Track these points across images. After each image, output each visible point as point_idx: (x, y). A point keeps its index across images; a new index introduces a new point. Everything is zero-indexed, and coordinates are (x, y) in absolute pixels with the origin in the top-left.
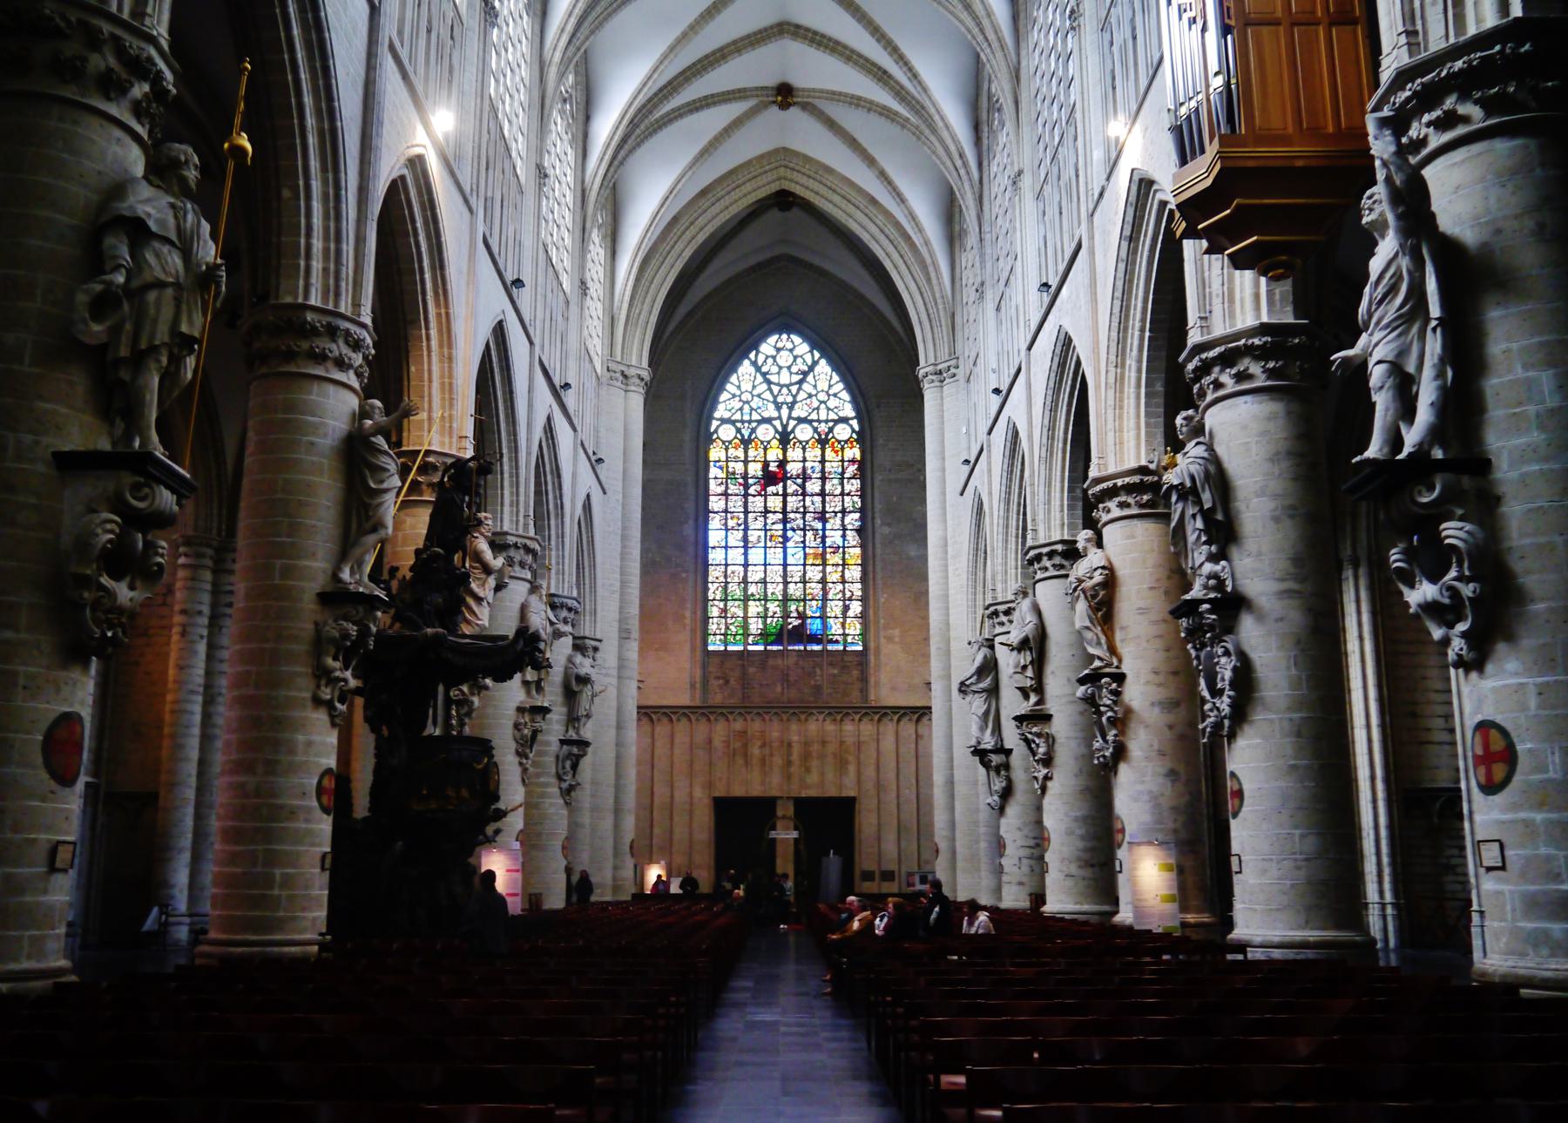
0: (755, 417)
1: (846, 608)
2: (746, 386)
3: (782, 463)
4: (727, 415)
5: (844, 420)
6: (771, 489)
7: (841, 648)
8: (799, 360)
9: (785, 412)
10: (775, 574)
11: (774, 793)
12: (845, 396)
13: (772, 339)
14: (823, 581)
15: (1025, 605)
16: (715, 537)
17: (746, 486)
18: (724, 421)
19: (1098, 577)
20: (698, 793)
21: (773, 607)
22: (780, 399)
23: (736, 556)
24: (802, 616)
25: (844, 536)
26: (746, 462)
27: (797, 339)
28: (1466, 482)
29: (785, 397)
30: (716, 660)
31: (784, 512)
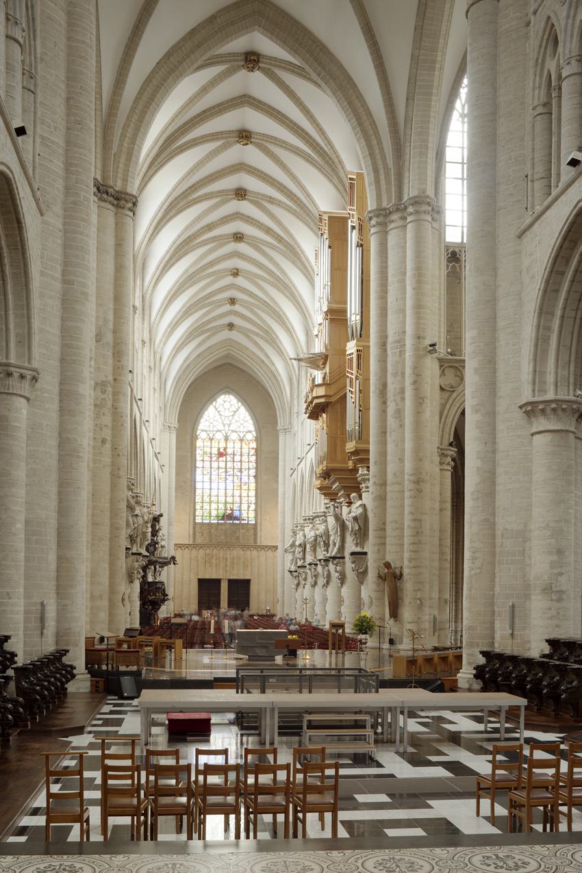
0: (215, 429)
1: (249, 507)
2: (212, 416)
3: (225, 449)
4: (203, 428)
5: (250, 432)
6: (221, 459)
7: (246, 522)
8: (233, 406)
9: (227, 427)
10: (222, 492)
11: (220, 578)
12: (251, 422)
13: (222, 397)
14: (240, 496)
15: (301, 533)
16: (199, 477)
17: (211, 457)
18: (202, 431)
19: (313, 539)
20: (192, 576)
21: (221, 506)
22: (225, 422)
23: (207, 485)
24: (232, 510)
25: (249, 479)
26: (211, 447)
27: (232, 397)
28: (341, 560)
29: (227, 421)
30: (199, 526)
31: (226, 468)
